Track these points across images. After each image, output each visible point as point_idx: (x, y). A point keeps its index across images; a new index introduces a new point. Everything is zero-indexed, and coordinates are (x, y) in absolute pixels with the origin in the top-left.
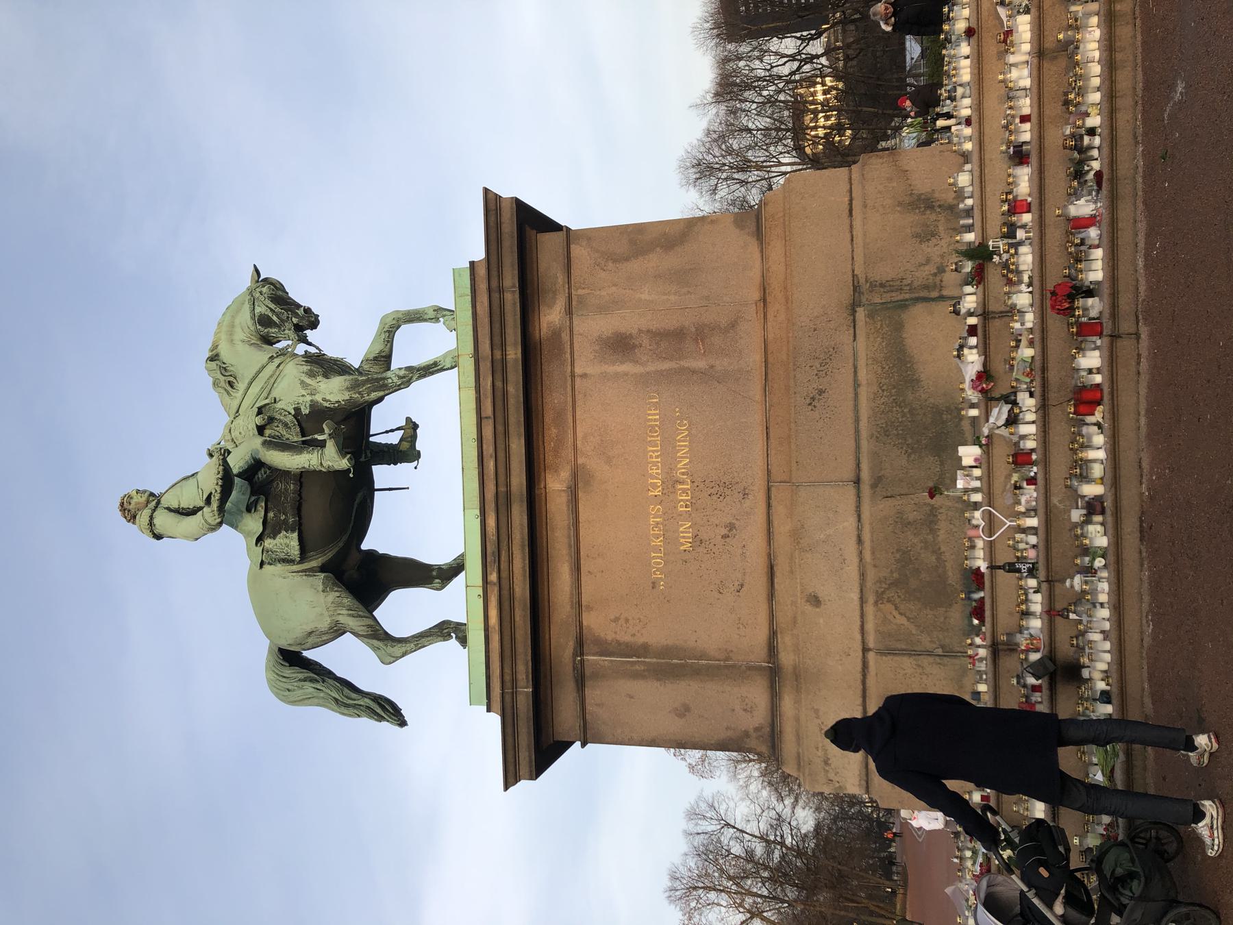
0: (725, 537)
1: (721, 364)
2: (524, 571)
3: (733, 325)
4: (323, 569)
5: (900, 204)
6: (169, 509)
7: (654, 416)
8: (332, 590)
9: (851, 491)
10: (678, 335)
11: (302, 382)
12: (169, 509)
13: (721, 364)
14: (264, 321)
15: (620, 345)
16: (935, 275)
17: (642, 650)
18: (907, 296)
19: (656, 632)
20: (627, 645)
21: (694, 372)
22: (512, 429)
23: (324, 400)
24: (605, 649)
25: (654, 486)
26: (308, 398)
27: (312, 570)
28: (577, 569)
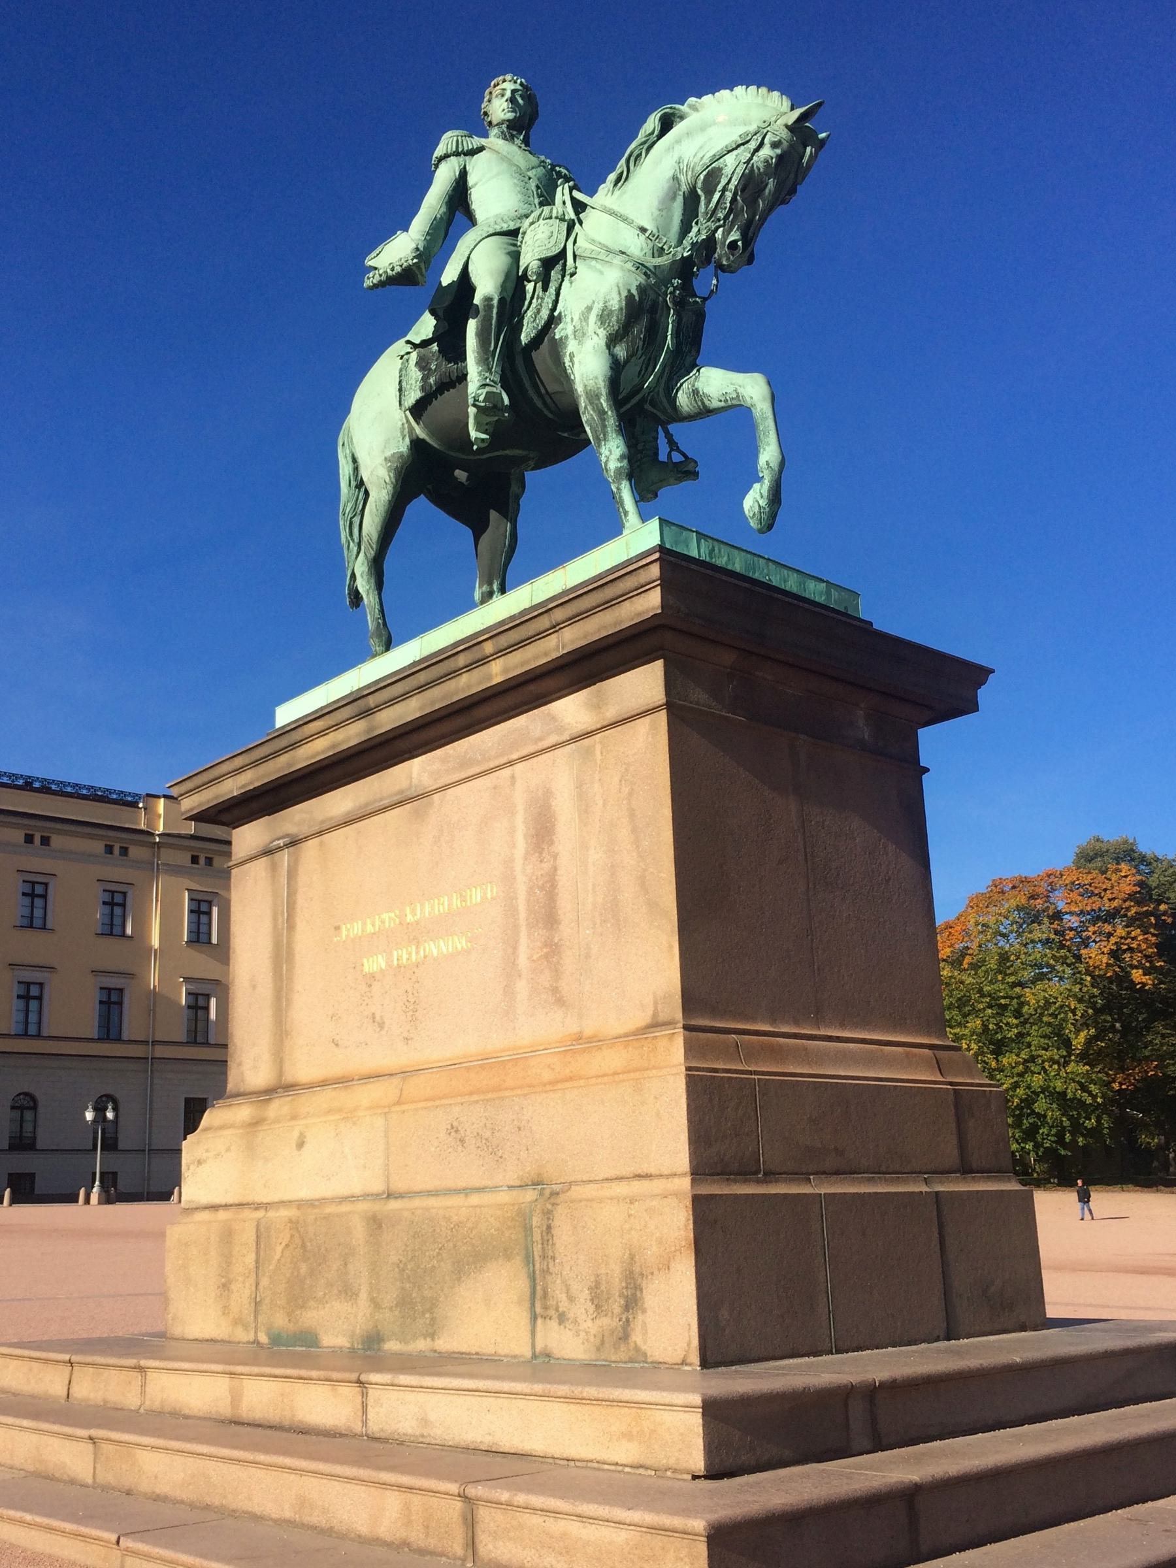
1: (522, 987)
2: (313, 757)
3: (560, 1002)
4: (417, 444)
5: (632, 1257)
8: (389, 471)
9: (378, 1186)
11: (589, 309)
12: (464, 173)
13: (522, 987)
14: (712, 176)
16: (557, 1310)
17: (291, 927)
18: (537, 1266)
20: (295, 903)
23: (572, 356)
24: (292, 874)
25: (414, 913)
27: (411, 429)
28: (349, 821)
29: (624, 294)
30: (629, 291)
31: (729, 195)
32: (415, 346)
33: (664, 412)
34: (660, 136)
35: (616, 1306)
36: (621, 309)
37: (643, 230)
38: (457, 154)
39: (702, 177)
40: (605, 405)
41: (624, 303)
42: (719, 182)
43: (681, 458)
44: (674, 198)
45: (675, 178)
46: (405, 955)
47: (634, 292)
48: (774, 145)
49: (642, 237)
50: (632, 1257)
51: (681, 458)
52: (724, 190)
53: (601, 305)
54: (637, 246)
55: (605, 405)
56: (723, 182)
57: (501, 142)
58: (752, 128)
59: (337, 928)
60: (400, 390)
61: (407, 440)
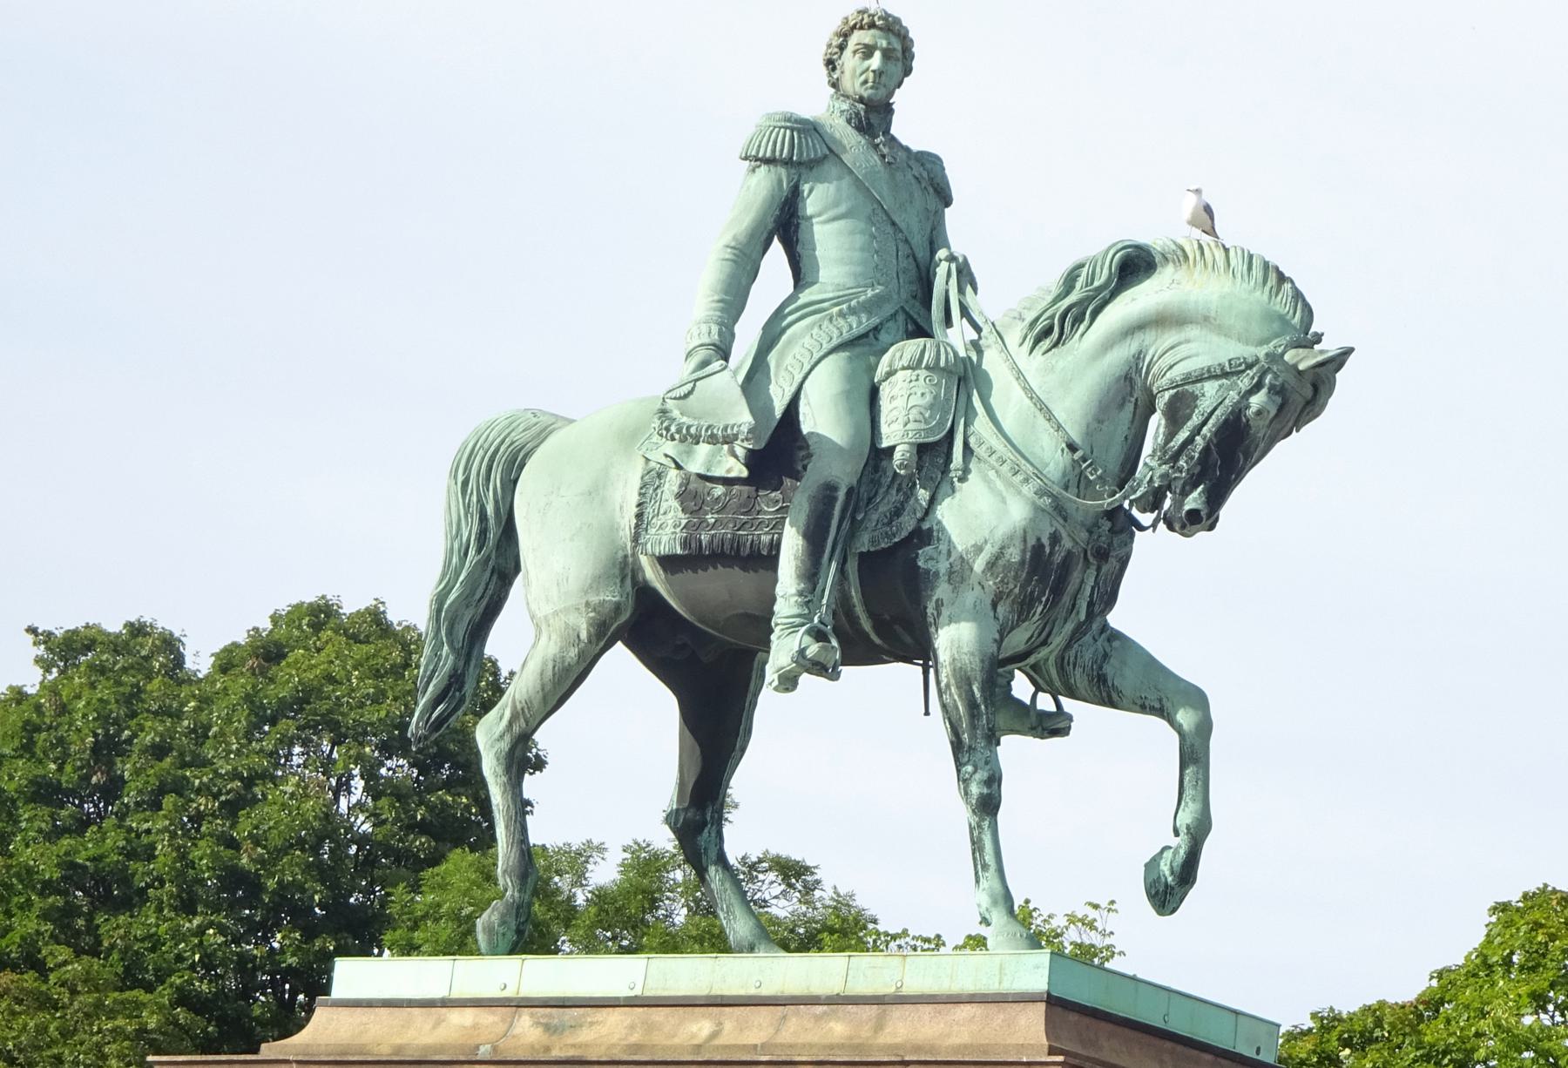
23: (939, 604)
26: (943, 567)
29: (1031, 542)
30: (1039, 539)
32: (679, 467)
33: (1050, 683)
34: (1114, 295)
36: (1022, 562)
37: (1072, 447)
38: (788, 163)
39: (1167, 395)
40: (978, 694)
41: (1028, 555)
42: (1189, 417)
43: (1052, 708)
44: (1122, 406)
47: (1045, 541)
49: (1068, 455)
51: (1052, 708)
52: (1197, 430)
53: (996, 549)
55: (978, 694)
56: (1196, 420)
60: (639, 516)
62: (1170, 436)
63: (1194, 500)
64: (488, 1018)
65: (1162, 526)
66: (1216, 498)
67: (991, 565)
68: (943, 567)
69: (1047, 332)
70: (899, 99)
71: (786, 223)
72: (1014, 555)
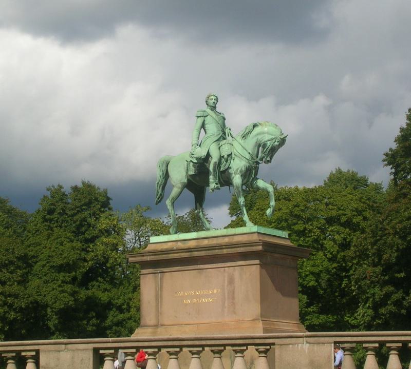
0: (187, 313)
3: (235, 313)
5: (252, 357)
6: (204, 121)
7: (215, 291)
10: (233, 298)
11: (238, 169)
12: (204, 121)
14: (264, 146)
15: (231, 281)
19: (166, 294)
21: (225, 302)
22: (208, 251)
23: (233, 178)
26: (233, 172)
31: (268, 150)
35: (249, 364)
37: (250, 153)
38: (203, 116)
45: (256, 142)
46: (196, 300)
48: (278, 142)
50: (252, 357)
54: (248, 156)
57: (210, 111)
58: (273, 137)
59: (176, 293)
61: (186, 179)
62: (263, 150)
63: (268, 159)
64: (174, 243)
65: (263, 163)
66: (271, 158)
67: (241, 171)
68: (233, 172)
69: (244, 137)
70: (217, 106)
71: (203, 126)
72: (244, 169)
